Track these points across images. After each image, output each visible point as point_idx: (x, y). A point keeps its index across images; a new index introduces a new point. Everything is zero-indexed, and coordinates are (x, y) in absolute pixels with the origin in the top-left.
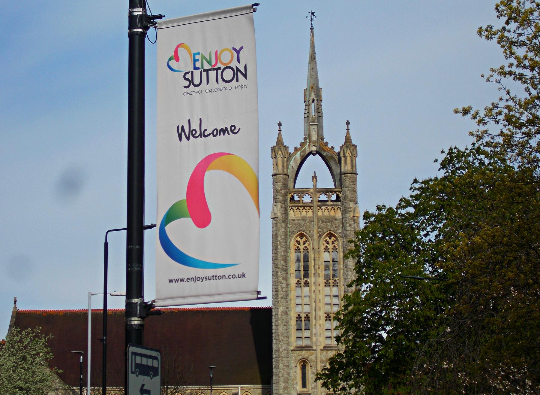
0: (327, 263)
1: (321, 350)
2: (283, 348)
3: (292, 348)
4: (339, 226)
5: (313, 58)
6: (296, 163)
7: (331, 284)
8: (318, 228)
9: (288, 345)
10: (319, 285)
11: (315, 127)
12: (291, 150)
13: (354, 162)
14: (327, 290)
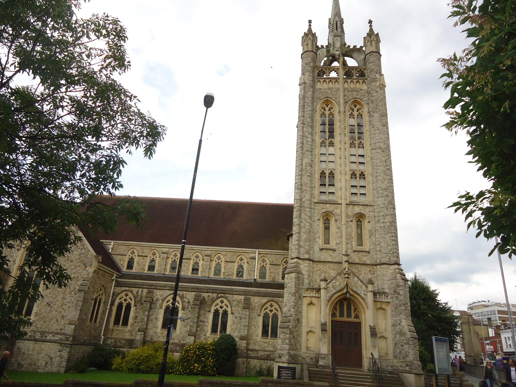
0: (352, 127)
3: (316, 201)
7: (357, 145)
10: (345, 143)
11: (339, 38)
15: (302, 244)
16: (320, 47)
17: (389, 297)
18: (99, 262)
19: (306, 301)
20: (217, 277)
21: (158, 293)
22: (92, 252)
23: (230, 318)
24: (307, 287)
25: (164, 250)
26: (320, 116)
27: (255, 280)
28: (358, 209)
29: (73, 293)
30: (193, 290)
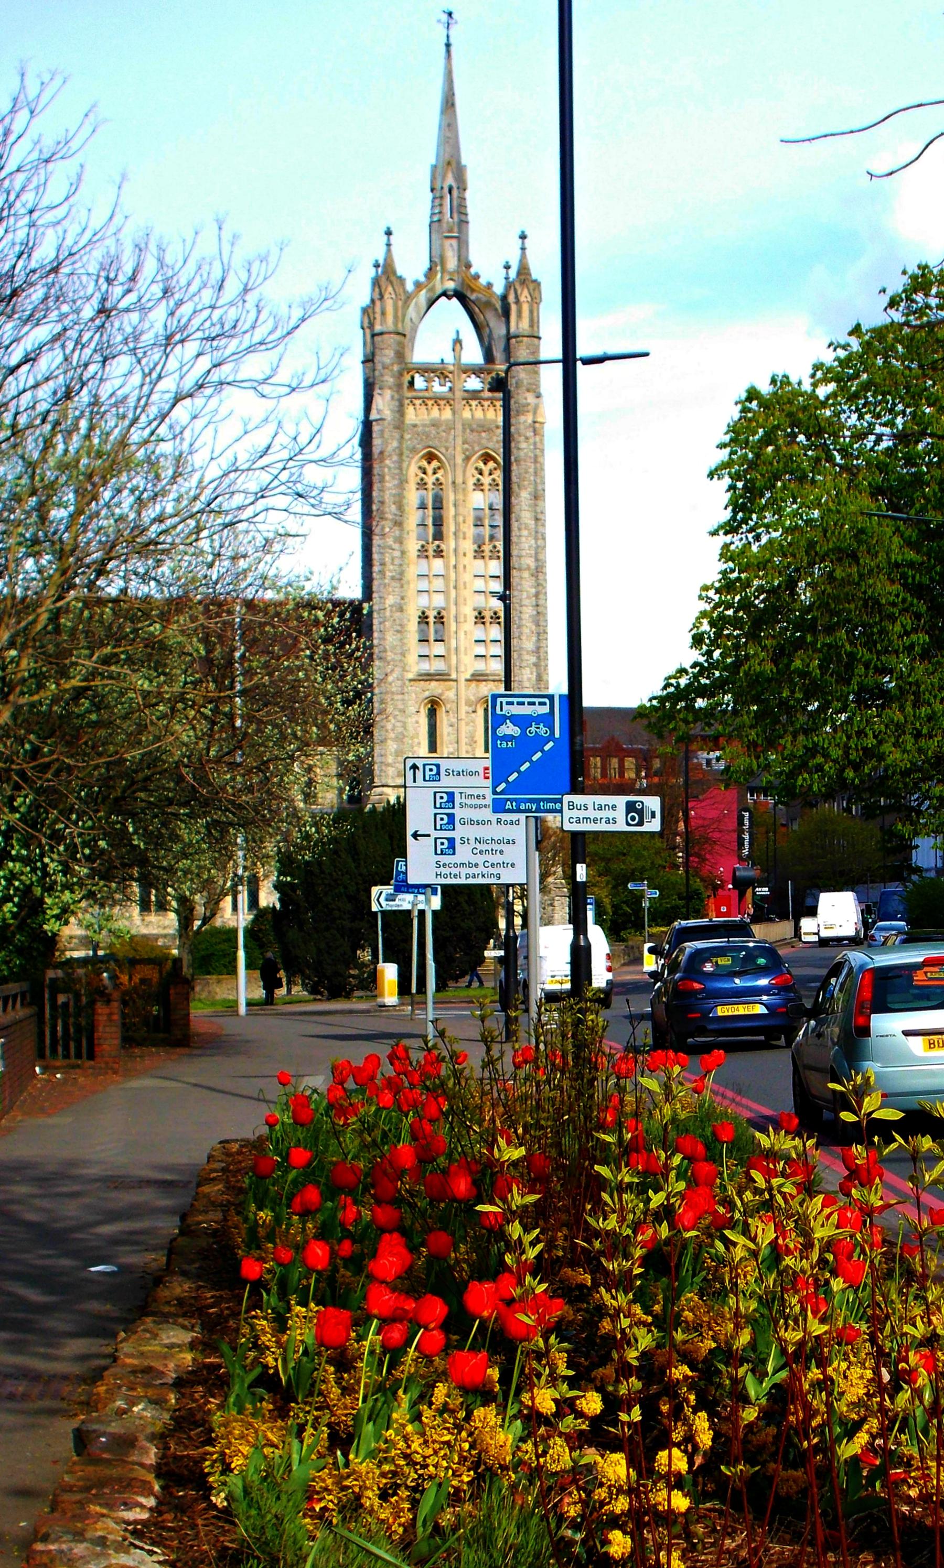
3: (411, 676)
5: (449, 104)
6: (418, 312)
7: (487, 554)
9: (404, 670)
11: (454, 242)
12: (410, 287)
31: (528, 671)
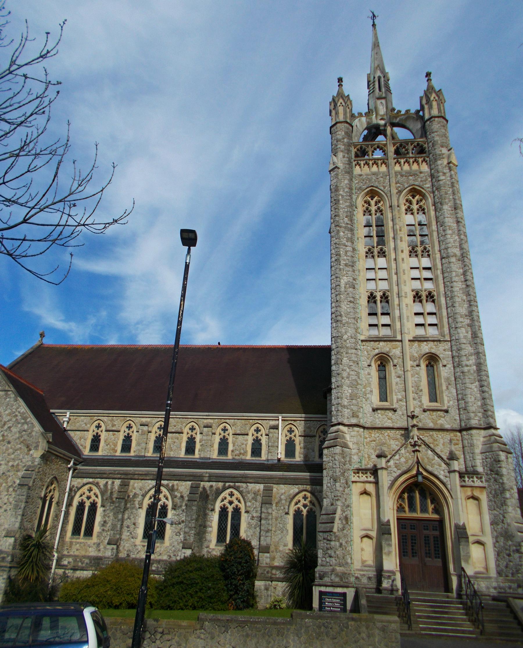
1: (409, 341)
2: (349, 334)
3: (363, 338)
4: (426, 180)
5: (376, 45)
6: (361, 124)
7: (419, 253)
8: (396, 184)
10: (402, 251)
11: (383, 101)
13: (442, 108)
14: (414, 262)
15: (346, 404)
16: (356, 115)
17: (483, 479)
18: (48, 442)
19: (356, 489)
20: (223, 458)
21: (136, 485)
22: (38, 428)
23: (244, 518)
24: (357, 466)
25: (144, 420)
26: (361, 213)
27: (279, 460)
28: (426, 348)
29: (11, 489)
30: (188, 478)
31: (463, 330)
